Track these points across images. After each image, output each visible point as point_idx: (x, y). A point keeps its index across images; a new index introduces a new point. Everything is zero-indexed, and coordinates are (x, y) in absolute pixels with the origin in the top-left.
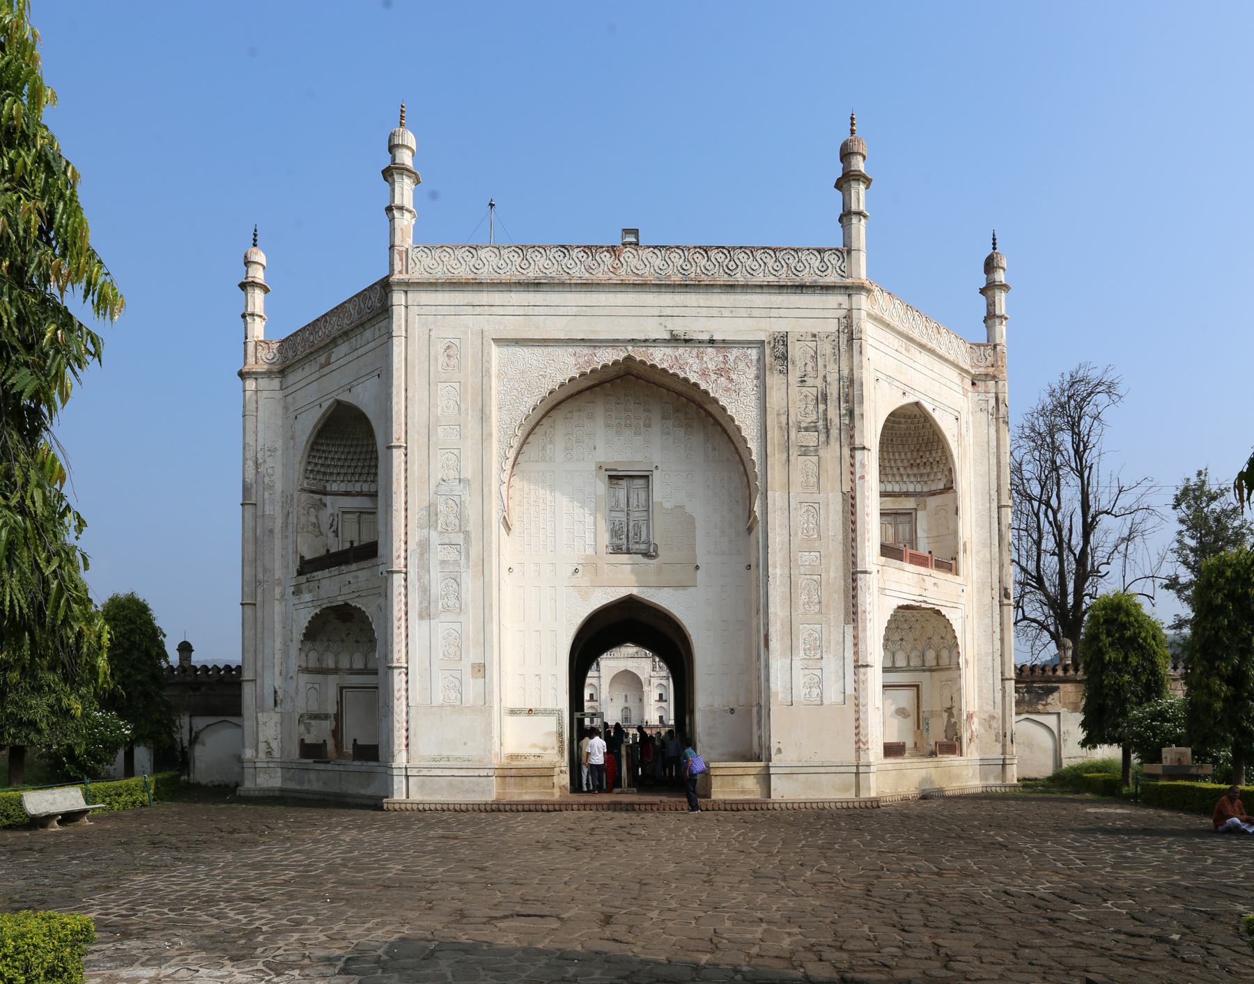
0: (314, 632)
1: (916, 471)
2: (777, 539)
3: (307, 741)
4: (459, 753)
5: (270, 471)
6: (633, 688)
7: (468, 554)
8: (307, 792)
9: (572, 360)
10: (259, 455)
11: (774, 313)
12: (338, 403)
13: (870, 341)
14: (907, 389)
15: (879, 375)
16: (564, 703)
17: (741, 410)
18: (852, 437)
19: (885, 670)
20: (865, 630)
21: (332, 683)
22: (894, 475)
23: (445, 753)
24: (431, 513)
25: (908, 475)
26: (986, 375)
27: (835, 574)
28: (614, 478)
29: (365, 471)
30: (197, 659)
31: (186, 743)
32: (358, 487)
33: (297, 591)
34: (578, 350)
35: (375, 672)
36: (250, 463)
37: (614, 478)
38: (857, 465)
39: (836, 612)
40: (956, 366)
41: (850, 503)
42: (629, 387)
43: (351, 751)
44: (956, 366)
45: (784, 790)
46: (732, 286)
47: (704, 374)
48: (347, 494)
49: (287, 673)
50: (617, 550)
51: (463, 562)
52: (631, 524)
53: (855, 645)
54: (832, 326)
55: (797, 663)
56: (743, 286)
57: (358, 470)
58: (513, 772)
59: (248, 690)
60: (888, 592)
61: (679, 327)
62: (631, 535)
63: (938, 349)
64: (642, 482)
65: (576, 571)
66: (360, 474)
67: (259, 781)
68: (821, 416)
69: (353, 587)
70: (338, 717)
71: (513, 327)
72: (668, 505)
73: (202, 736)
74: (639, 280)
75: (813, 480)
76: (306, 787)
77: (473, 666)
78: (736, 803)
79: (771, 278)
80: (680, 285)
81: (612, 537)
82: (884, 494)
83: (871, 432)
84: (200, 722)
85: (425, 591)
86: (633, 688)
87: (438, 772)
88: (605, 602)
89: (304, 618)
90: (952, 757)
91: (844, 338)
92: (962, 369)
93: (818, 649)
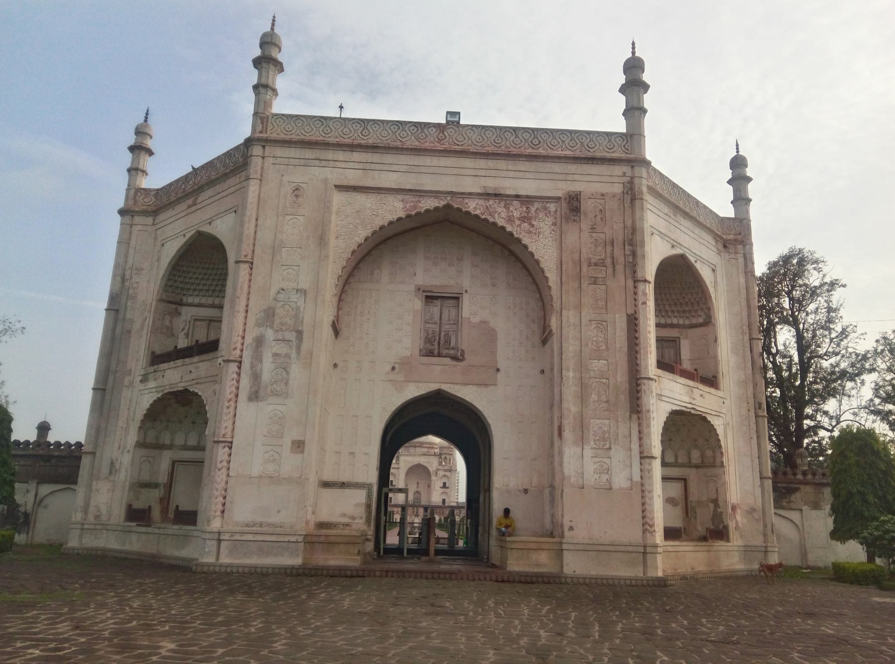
1: (680, 309)
2: (571, 348)
3: (135, 506)
5: (135, 285)
7: (299, 349)
8: (127, 552)
9: (400, 205)
12: (199, 233)
14: (675, 244)
17: (543, 246)
18: (635, 272)
20: (649, 426)
24: (269, 315)
26: (736, 240)
27: (621, 377)
33: (145, 379)
37: (430, 298)
38: (640, 293)
39: (623, 411)
41: (633, 323)
42: (444, 227)
45: (575, 565)
48: (200, 305)
49: (124, 448)
50: (430, 354)
52: (443, 334)
53: (640, 439)
55: (588, 452)
59: (86, 461)
60: (664, 398)
62: (442, 342)
64: (453, 302)
65: (393, 368)
66: (214, 291)
67: (84, 541)
68: (609, 254)
70: (169, 486)
71: (352, 177)
72: (475, 320)
75: (601, 303)
76: (127, 547)
81: (426, 343)
89: (147, 401)
92: (717, 235)
93: (605, 445)
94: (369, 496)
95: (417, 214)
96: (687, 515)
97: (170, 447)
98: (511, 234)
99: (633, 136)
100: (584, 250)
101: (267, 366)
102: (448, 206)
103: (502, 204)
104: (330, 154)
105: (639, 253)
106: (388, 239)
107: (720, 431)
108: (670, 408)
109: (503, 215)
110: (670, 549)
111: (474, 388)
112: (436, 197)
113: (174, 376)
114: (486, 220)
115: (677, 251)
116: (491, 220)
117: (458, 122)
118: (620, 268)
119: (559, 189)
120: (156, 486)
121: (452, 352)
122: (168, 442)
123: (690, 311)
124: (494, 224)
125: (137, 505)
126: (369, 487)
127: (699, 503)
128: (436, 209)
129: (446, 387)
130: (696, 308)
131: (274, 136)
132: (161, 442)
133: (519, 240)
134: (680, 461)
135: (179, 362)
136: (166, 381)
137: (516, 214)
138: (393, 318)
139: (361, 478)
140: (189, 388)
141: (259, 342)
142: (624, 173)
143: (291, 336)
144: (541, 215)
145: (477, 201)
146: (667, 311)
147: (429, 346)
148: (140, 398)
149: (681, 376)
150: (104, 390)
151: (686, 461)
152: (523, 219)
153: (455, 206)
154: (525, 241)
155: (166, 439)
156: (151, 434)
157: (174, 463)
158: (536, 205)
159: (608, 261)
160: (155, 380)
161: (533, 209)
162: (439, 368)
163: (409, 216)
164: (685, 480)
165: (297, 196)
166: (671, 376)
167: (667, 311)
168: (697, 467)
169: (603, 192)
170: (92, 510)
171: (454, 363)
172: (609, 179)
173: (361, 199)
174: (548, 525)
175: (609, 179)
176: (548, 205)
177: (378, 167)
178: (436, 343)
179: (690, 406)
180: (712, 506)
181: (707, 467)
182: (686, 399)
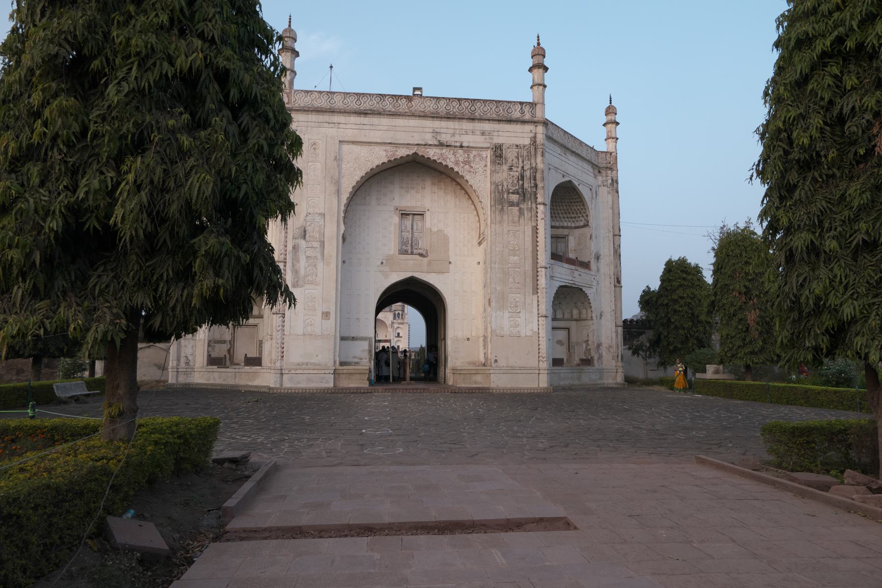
4: (313, 361)
6: (408, 330)
19: (553, 320)
23: (306, 361)
28: (404, 215)
37: (404, 215)
50: (403, 252)
58: (345, 371)
65: (382, 263)
72: (435, 229)
77: (323, 313)
78: (472, 389)
81: (402, 245)
83: (544, 196)
86: (408, 330)
88: (398, 280)
94: (370, 346)
98: (457, 173)
100: (505, 184)
101: (302, 263)
102: (415, 154)
103: (452, 152)
104: (336, 118)
105: (540, 185)
108: (558, 284)
109: (453, 159)
111: (435, 275)
114: (441, 163)
115: (567, 179)
116: (444, 163)
121: (420, 251)
124: (446, 166)
127: (577, 343)
128: (408, 156)
129: (417, 275)
133: (462, 177)
137: (461, 159)
141: (295, 248)
143: (316, 244)
144: (477, 159)
147: (404, 247)
152: (467, 162)
154: (467, 177)
158: (474, 153)
161: (472, 156)
163: (389, 161)
165: (315, 149)
166: (560, 263)
168: (576, 320)
169: (518, 143)
171: (421, 258)
172: (521, 135)
173: (356, 148)
174: (482, 360)
175: (521, 135)
180: (584, 345)
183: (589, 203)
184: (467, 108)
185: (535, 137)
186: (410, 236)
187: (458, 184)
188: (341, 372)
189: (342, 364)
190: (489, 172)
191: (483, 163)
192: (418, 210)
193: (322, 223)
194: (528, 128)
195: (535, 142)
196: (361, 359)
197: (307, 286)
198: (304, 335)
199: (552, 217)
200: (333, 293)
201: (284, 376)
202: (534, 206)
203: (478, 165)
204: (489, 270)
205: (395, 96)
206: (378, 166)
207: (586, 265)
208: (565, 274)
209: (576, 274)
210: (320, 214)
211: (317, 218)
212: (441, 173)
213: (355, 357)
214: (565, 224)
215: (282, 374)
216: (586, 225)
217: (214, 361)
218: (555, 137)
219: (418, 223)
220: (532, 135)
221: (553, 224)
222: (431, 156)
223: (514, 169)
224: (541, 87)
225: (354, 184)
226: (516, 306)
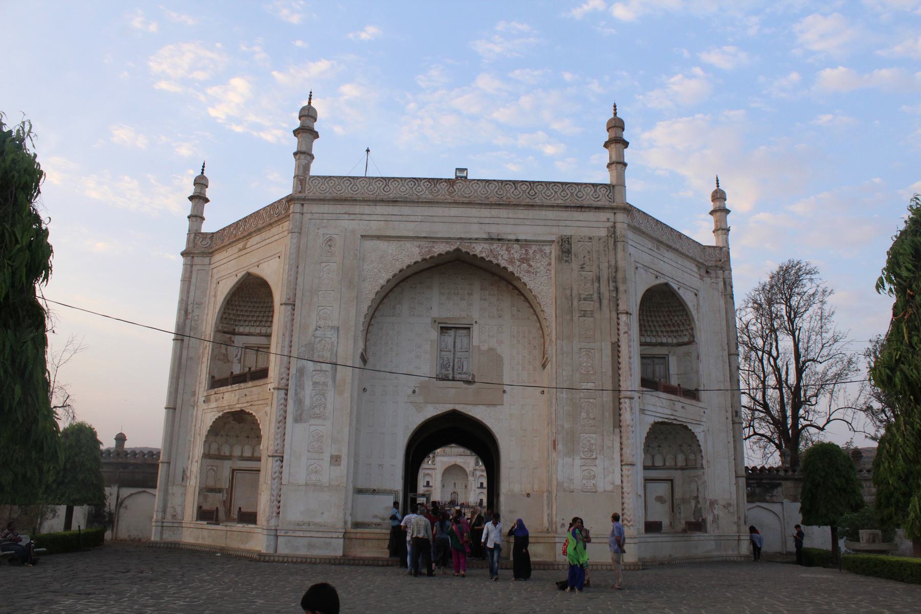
0: (216, 430)
10: (190, 308)
11: (561, 223)
13: (630, 242)
15: (638, 265)
16: (397, 483)
21: (227, 466)
22: (652, 331)
23: (307, 520)
25: (662, 332)
29: (265, 319)
30: (128, 445)
31: (113, 507)
32: (258, 330)
34: (422, 243)
35: (259, 459)
36: (183, 312)
37: (444, 329)
40: (693, 259)
43: (236, 516)
44: (695, 260)
46: (532, 206)
47: (511, 261)
51: (330, 383)
54: (603, 233)
56: (539, 206)
57: (260, 319)
59: (162, 470)
61: (494, 230)
62: (456, 367)
63: (680, 249)
64: (465, 331)
65: (414, 392)
67: (165, 536)
69: (248, 398)
72: (485, 348)
73: (126, 502)
74: (466, 200)
77: (332, 457)
79: (560, 201)
80: (495, 204)
82: (642, 344)
84: (126, 492)
85: (299, 402)
87: (301, 534)
88: (435, 414)
90: (698, 534)
91: (611, 241)
95: (431, 258)
96: (673, 511)
97: (229, 458)
98: (512, 273)
99: (615, 188)
101: (308, 392)
102: (458, 250)
103: (504, 248)
104: (358, 209)
105: (622, 288)
106: (408, 277)
107: (700, 437)
108: (651, 420)
109: (506, 257)
110: (648, 540)
111: (484, 408)
112: (447, 243)
113: (231, 398)
114: (491, 262)
115: (661, 281)
116: (495, 262)
117: (466, 178)
118: (605, 302)
119: (550, 233)
120: (220, 491)
121: (464, 376)
122: (228, 453)
123: (677, 331)
124: (498, 265)
125: (206, 507)
126: (396, 493)
128: (448, 253)
129: (459, 408)
130: (682, 328)
131: (311, 195)
132: (222, 453)
133: (519, 279)
134: (667, 464)
135: (236, 386)
136: (225, 403)
137: (516, 256)
138: (414, 347)
139: (387, 486)
140: (244, 409)
142: (608, 219)
145: (483, 245)
146: (657, 332)
147: (444, 371)
148: (206, 415)
149: (664, 392)
150: (175, 409)
151: (673, 464)
153: (464, 250)
154: (525, 279)
155: (226, 451)
156: (214, 446)
157: (233, 470)
158: (534, 248)
159: (595, 296)
160: (216, 401)
161: (531, 252)
162: (453, 391)
163: (424, 260)
164: (672, 481)
165: (330, 246)
167: (657, 332)
168: (682, 469)
169: (591, 235)
170: (169, 511)
171: (466, 386)
172: (595, 225)
173: (382, 245)
174: (546, 524)
176: (544, 247)
177: (398, 218)
178: (450, 369)
179: (672, 417)
180: (693, 502)
181: (690, 469)
182: (669, 412)
183: (694, 312)
184: (524, 192)
185: (614, 227)
186: (452, 357)
187: (516, 288)
188: (353, 536)
189: (356, 525)
190: (553, 272)
191: (545, 261)
192: (464, 322)
193: (334, 339)
194: (603, 216)
195: (614, 233)
196: (384, 519)
197: (312, 421)
198: (307, 485)
199: (641, 330)
200: (346, 430)
201: (280, 540)
202: (614, 315)
203: (539, 264)
204: (554, 401)
205: (433, 179)
206: (409, 266)
207: (693, 394)
208: (660, 407)
209: (678, 406)
210: (332, 328)
211: (329, 334)
212: (502, 278)
213: (376, 516)
214: (664, 340)
215: (277, 536)
216: (691, 342)
217: (206, 515)
218: (643, 227)
219: (462, 339)
220: (610, 224)
221: (643, 340)
222: (477, 252)
223: (587, 268)
224: (620, 166)
225: (378, 288)
226: (591, 451)
